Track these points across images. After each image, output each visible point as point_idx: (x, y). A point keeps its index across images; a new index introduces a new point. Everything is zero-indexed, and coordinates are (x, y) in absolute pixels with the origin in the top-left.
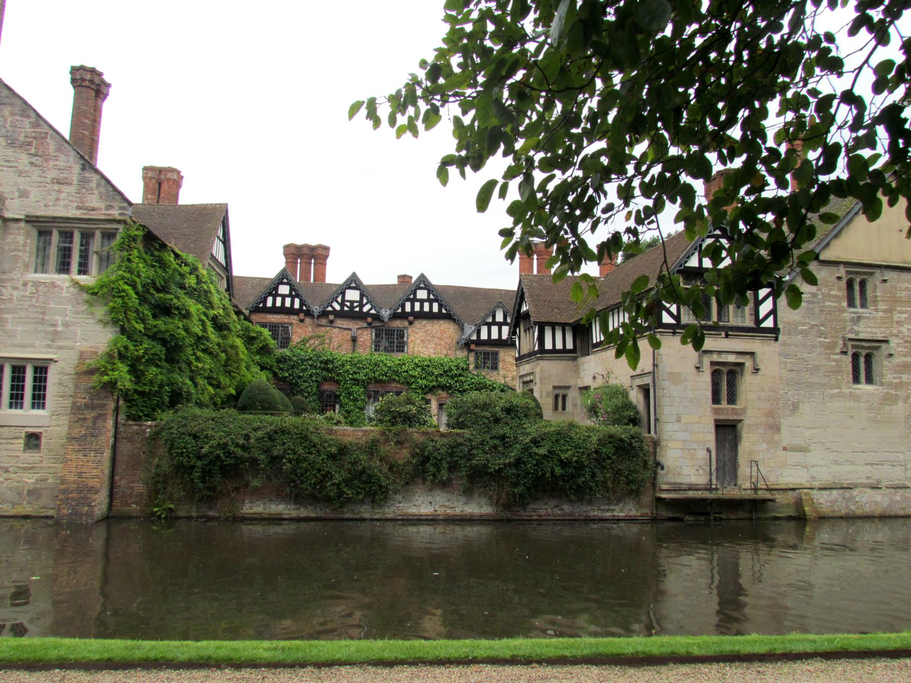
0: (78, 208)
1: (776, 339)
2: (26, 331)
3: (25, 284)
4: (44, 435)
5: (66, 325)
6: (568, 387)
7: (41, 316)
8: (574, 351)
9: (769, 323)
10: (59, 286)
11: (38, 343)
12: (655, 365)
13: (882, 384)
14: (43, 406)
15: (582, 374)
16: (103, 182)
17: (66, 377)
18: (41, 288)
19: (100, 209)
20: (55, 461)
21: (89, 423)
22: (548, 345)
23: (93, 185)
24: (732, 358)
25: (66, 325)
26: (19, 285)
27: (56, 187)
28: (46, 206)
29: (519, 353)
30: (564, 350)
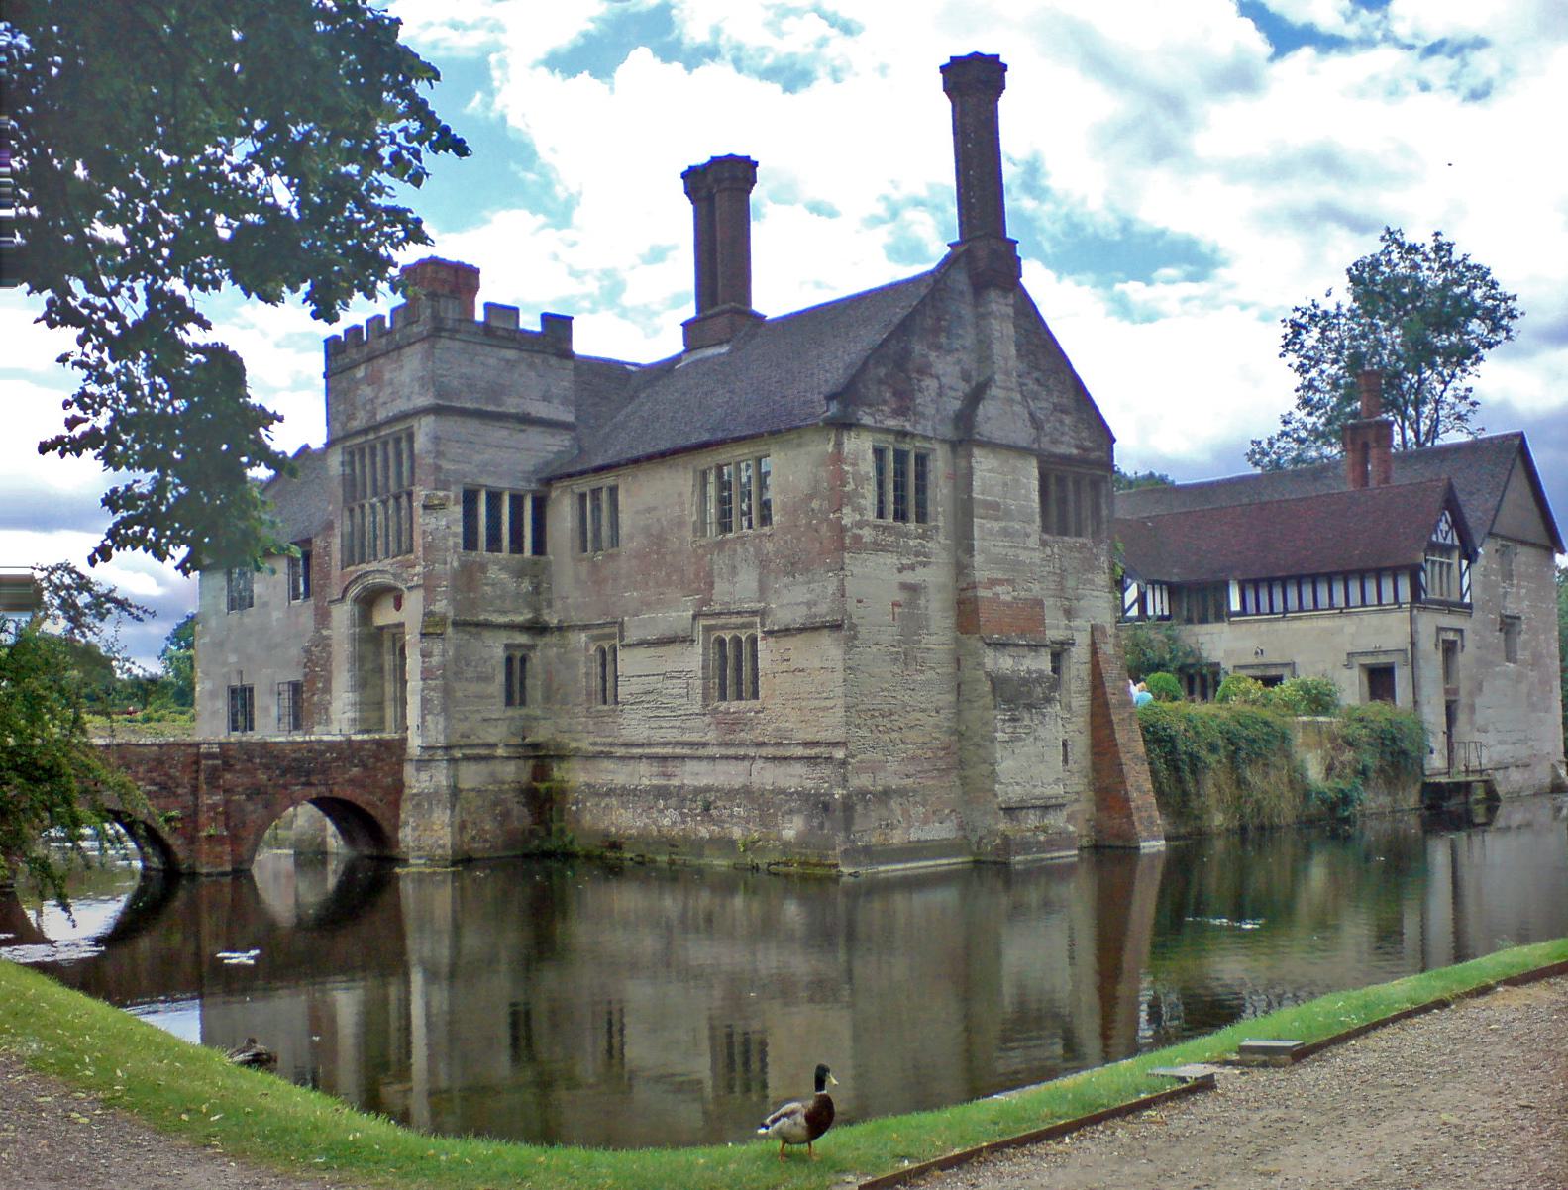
0: (1077, 447)
1: (1470, 614)
8: (1168, 618)
9: (1467, 600)
12: (1413, 644)
13: (1515, 662)
22: (1150, 612)
24: (1451, 636)
30: (1162, 618)
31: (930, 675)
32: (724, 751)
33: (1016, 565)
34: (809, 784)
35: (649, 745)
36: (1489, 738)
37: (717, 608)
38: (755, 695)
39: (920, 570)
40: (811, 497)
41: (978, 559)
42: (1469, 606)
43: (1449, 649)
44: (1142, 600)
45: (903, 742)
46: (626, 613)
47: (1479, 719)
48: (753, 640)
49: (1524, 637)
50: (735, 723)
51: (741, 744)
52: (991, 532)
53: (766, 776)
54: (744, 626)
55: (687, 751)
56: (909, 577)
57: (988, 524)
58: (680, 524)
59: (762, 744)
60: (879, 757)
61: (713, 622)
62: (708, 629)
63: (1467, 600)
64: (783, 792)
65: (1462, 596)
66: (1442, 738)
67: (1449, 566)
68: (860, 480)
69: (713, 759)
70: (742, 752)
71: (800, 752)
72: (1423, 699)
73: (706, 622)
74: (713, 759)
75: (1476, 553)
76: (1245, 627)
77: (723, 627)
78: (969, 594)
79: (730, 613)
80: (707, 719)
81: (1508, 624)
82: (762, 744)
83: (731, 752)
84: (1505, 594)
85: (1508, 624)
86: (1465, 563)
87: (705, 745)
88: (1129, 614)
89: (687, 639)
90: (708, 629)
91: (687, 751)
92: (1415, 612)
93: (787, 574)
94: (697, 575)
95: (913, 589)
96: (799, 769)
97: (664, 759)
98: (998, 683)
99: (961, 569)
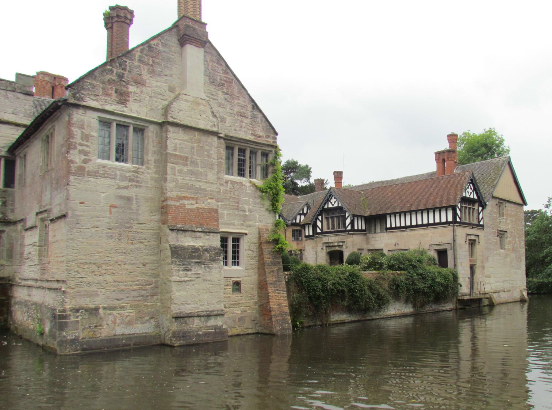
2: (229, 214)
3: (227, 182)
4: (242, 282)
5: (250, 211)
6: (362, 249)
7: (237, 205)
8: (365, 231)
9: (481, 223)
10: (245, 185)
11: (236, 222)
13: (505, 249)
14: (237, 264)
15: (373, 243)
16: (264, 119)
17: (252, 245)
18: (235, 186)
19: (263, 137)
20: (247, 298)
21: (275, 274)
22: (356, 228)
23: (259, 120)
25: (250, 211)
26: (224, 182)
27: (239, 118)
28: (235, 130)
29: (322, 230)
30: (362, 230)
31: (138, 245)
33: (199, 190)
36: (492, 280)
39: (135, 189)
41: (169, 185)
42: (483, 226)
43: (472, 243)
44: (352, 223)
45: (115, 281)
47: (486, 272)
49: (509, 239)
52: (181, 171)
56: (124, 193)
57: (177, 167)
60: (95, 289)
63: (481, 223)
65: (479, 222)
66: (468, 280)
67: (474, 209)
68: (86, 137)
72: (459, 264)
75: (486, 205)
76: (392, 234)
78: (165, 203)
81: (501, 234)
84: (500, 222)
85: (501, 234)
86: (480, 208)
88: (348, 229)
92: (455, 227)
95: (129, 199)
98: (176, 252)
99: (162, 190)
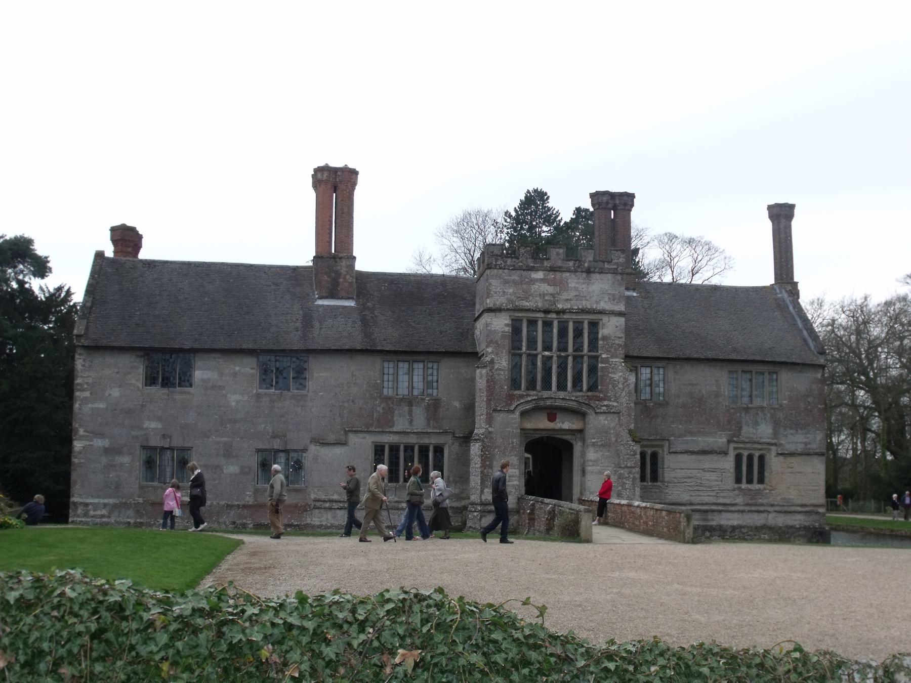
32: (747, 508)
34: (807, 524)
35: (691, 504)
37: (742, 438)
38: (761, 481)
40: (808, 396)
46: (672, 435)
48: (762, 458)
50: (758, 492)
51: (762, 505)
53: (781, 521)
54: (760, 450)
55: (720, 508)
58: (717, 395)
59: (772, 505)
61: (742, 446)
62: (735, 448)
64: (792, 527)
69: (743, 512)
70: (762, 509)
71: (799, 509)
73: (736, 445)
74: (743, 512)
77: (745, 449)
79: (755, 443)
80: (737, 492)
82: (772, 505)
83: (753, 508)
87: (735, 505)
89: (726, 453)
90: (735, 448)
91: (720, 508)
93: (791, 428)
94: (729, 422)
96: (799, 517)
97: (706, 511)
